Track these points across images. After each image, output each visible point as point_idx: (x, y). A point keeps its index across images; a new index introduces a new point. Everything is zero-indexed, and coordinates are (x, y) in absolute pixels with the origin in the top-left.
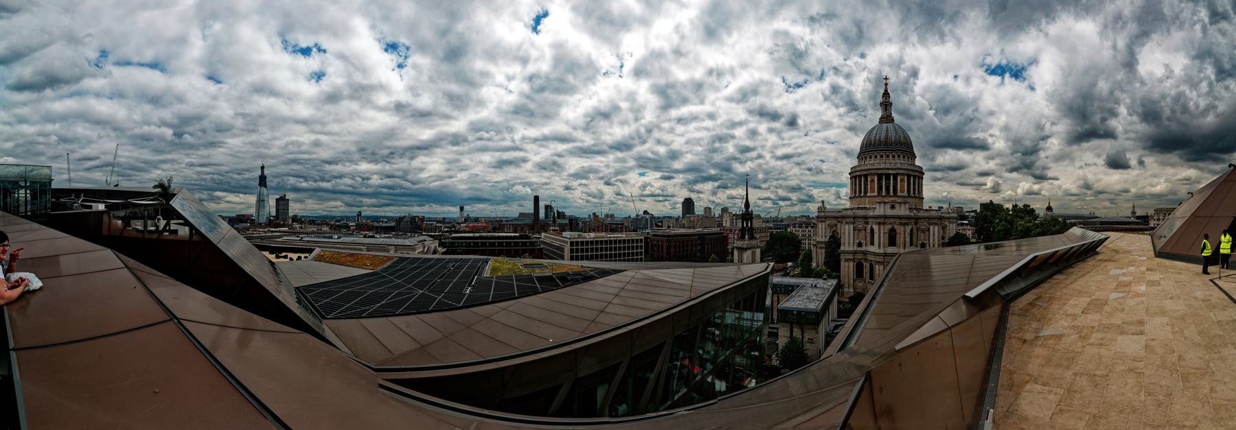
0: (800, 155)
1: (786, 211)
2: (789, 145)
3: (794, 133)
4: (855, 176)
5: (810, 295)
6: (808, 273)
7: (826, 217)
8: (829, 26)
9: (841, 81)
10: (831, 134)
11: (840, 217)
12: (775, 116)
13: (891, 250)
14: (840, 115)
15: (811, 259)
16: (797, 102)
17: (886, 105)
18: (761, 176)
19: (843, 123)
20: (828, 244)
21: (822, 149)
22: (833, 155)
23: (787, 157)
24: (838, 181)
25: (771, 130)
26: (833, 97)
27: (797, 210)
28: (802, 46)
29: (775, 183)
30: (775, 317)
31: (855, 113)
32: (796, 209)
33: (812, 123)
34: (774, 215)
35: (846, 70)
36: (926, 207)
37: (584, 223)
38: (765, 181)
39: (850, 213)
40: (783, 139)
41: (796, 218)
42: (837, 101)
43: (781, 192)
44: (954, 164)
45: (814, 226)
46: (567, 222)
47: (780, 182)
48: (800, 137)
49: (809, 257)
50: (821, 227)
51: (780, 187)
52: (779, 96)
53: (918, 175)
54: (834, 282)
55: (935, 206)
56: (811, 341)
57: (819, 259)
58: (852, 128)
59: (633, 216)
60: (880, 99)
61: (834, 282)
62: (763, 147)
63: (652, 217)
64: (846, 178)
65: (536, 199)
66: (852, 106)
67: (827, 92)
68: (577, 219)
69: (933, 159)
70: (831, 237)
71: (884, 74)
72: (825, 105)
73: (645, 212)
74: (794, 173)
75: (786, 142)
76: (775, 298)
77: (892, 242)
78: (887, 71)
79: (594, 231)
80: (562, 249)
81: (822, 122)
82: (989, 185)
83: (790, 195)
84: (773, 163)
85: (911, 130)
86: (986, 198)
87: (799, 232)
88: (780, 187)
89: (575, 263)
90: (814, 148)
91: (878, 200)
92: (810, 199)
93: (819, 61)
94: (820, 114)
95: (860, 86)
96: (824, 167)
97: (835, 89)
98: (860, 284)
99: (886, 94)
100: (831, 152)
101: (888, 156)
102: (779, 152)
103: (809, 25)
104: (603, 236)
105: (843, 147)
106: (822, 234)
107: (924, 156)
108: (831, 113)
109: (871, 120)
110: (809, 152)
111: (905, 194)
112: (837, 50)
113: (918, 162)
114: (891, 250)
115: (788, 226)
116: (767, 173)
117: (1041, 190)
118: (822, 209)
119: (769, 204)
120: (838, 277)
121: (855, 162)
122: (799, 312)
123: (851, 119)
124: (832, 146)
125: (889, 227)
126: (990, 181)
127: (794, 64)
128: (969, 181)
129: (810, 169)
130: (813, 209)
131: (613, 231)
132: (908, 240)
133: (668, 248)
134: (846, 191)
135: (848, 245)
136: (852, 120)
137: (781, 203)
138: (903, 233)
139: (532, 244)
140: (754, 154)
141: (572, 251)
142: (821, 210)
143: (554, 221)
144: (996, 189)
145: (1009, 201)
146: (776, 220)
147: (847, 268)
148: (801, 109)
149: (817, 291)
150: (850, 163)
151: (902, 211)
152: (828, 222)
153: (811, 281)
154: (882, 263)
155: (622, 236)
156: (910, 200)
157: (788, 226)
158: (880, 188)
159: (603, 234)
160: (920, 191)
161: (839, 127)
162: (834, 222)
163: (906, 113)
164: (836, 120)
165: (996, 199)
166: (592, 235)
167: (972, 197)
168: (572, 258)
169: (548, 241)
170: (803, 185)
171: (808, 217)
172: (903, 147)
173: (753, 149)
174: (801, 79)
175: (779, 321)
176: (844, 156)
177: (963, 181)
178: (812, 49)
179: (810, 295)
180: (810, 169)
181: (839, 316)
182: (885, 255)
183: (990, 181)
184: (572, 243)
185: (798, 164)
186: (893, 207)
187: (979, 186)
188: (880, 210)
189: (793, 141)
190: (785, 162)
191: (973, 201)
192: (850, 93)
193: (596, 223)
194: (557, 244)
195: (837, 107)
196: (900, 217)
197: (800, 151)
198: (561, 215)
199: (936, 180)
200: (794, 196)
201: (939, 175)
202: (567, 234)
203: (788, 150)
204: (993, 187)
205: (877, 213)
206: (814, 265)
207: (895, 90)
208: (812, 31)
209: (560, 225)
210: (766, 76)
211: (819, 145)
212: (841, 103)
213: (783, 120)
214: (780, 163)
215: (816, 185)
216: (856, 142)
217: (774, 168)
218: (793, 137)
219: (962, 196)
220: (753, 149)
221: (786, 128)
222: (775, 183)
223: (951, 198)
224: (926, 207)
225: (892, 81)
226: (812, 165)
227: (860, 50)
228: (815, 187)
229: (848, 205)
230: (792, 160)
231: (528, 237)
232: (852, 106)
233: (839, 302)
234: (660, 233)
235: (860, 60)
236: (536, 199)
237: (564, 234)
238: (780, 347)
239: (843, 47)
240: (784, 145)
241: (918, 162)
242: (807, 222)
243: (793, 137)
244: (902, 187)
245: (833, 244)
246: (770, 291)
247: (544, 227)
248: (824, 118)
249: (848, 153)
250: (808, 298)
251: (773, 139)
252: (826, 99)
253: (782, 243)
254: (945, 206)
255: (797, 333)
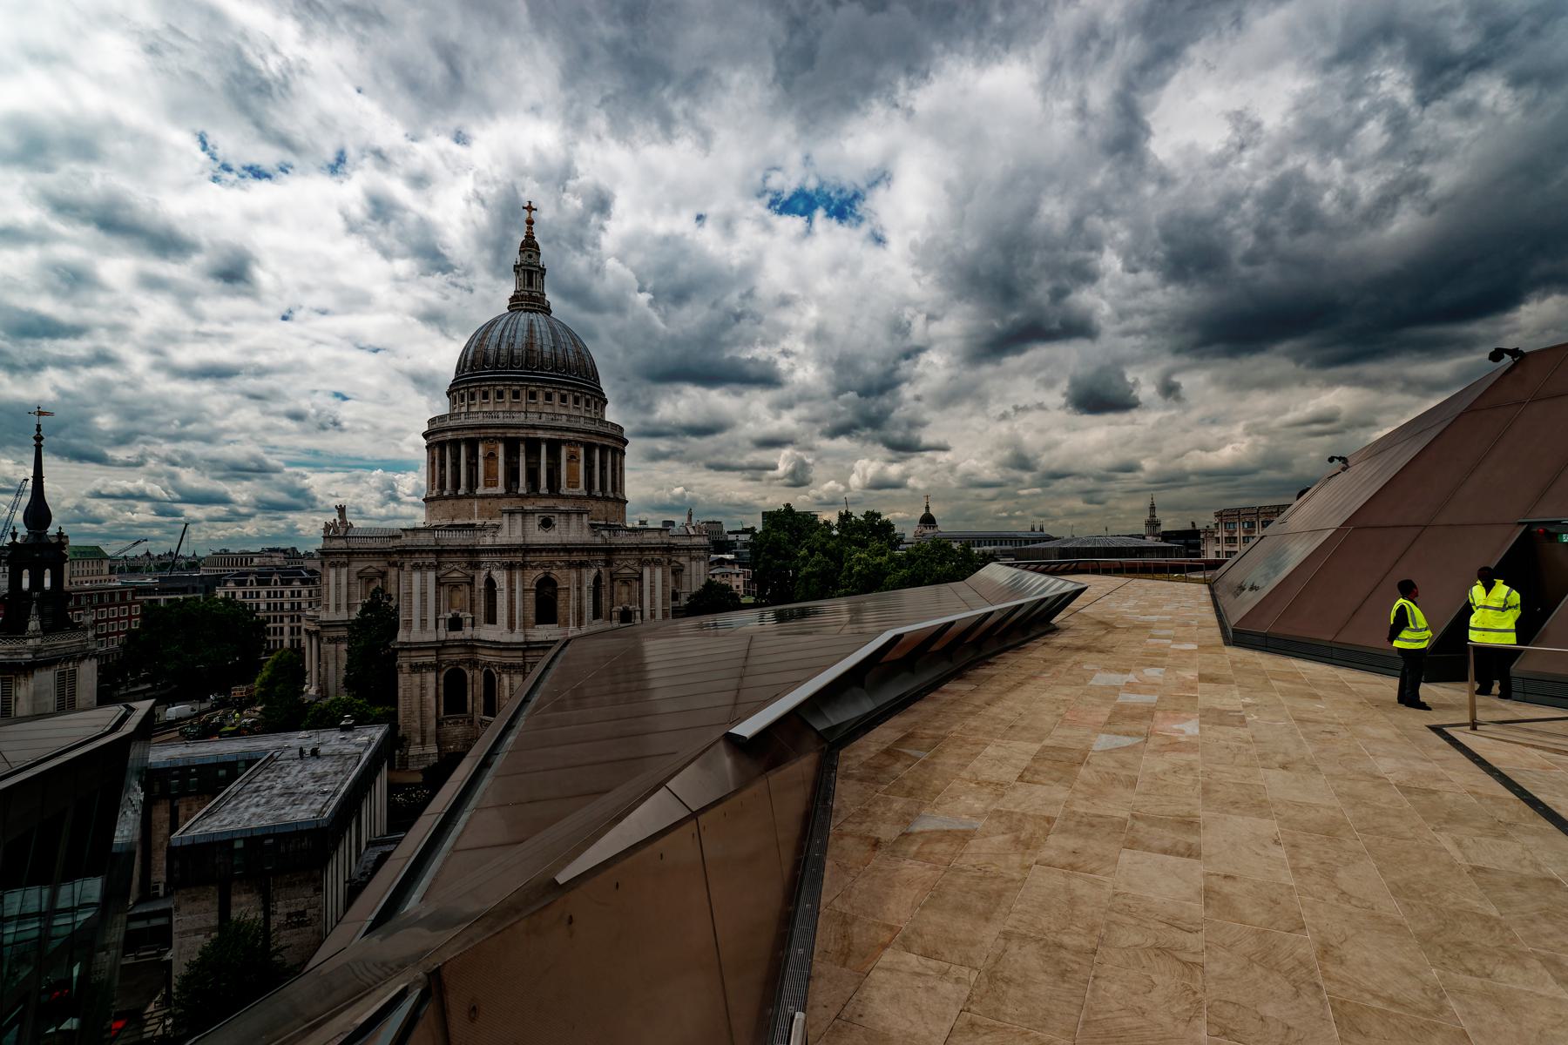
0: (261, 372)
1: (208, 534)
2: (225, 338)
3: (242, 305)
4: (440, 440)
5: (296, 779)
6: (288, 712)
7: (351, 554)
8: (362, 40)
9: (398, 189)
10: (369, 324)
11: (396, 551)
12: (167, 243)
13: (542, 633)
14: (396, 279)
15: (299, 676)
16: (252, 218)
17: (530, 271)
18: (105, 421)
19: (405, 301)
20: (356, 629)
21: (341, 363)
22: (373, 381)
23: (216, 373)
24: (390, 454)
25: (152, 284)
26: (374, 227)
27: (253, 532)
28: (272, 66)
29: (166, 448)
30: (160, 876)
31: (438, 279)
32: (250, 528)
33: (306, 289)
34: (159, 548)
35: (416, 164)
36: (632, 521)
38: (123, 439)
39: (424, 540)
40: (199, 318)
41: (247, 557)
42: (384, 239)
43: (189, 478)
44: (699, 419)
45: (312, 578)
47: (184, 446)
48: (263, 320)
49: (292, 668)
50: (336, 581)
51: (188, 460)
52: (186, 186)
53: (612, 444)
54: (377, 733)
55: (655, 521)
56: (298, 920)
57: (324, 673)
58: (433, 318)
60: (514, 256)
61: (377, 733)
62: (117, 329)
64: (415, 447)
66: (432, 257)
67: (357, 211)
69: (649, 409)
70: (366, 608)
71: (525, 197)
72: (352, 244)
74: (241, 425)
75: (217, 328)
76: (161, 814)
77: (546, 610)
78: (531, 191)
81: (339, 289)
82: (783, 467)
83: (222, 487)
84: (159, 385)
85: (593, 336)
86: (775, 499)
87: (261, 599)
88: (188, 460)
90: (314, 356)
91: (506, 505)
92: (302, 500)
93: (327, 122)
94: (330, 266)
95: (455, 214)
96: (346, 412)
97: (381, 208)
98: (458, 731)
99: (529, 245)
100: (365, 373)
101: (530, 396)
102: (186, 355)
103: (297, 17)
105: (407, 365)
106: (339, 598)
107: (626, 400)
108: (366, 268)
109: (486, 301)
110: (296, 368)
111: (581, 489)
112: (388, 108)
113: (611, 415)
114: (542, 633)
115: (219, 580)
116: (131, 412)
117: (906, 476)
118: (339, 529)
119: (143, 513)
120: (391, 718)
121: (442, 406)
122: (255, 841)
123: (430, 291)
124: (372, 359)
125: (539, 573)
126: (784, 460)
127: (244, 108)
128: (734, 460)
129: (297, 416)
130: (309, 529)
132: (588, 603)
134: (413, 482)
135: (420, 624)
136: (433, 297)
137: (191, 511)
138: (575, 586)
140: (77, 348)
142: (330, 532)
144: (799, 478)
145: (831, 504)
146: (168, 563)
147: (418, 691)
148: (262, 240)
149: (318, 767)
150: (424, 408)
151: (572, 532)
152: (357, 566)
153: (298, 739)
154: (522, 669)
156: (593, 506)
157: (219, 580)
158: (512, 475)
160: (618, 484)
161: (392, 309)
162: (378, 564)
163: (579, 295)
164: (382, 291)
165: (801, 501)
167: (743, 498)
170: (272, 461)
171: (292, 554)
172: (576, 377)
173: (76, 331)
174: (267, 156)
175: (173, 886)
176: (410, 389)
177: (721, 459)
178: (301, 84)
179: (296, 779)
180: (297, 416)
181: (390, 831)
182: (528, 647)
183: (784, 460)
185: (255, 397)
186: (546, 524)
187: (758, 471)
188: (511, 533)
189: (235, 328)
190: (206, 386)
191: (745, 507)
192: (424, 225)
195: (387, 254)
196: (567, 549)
197: (263, 359)
199: (656, 456)
200: (242, 492)
201: (662, 445)
203: (222, 354)
204: (793, 474)
205: (503, 538)
206: (311, 691)
207: (553, 239)
208: (308, 33)
210: (134, 114)
211: (329, 352)
212: (399, 247)
213: (198, 260)
214: (184, 390)
215: (318, 461)
216: (445, 356)
217: (165, 403)
218: (239, 318)
219: (720, 497)
220: (76, 331)
221: (213, 285)
222: (166, 448)
223: (694, 501)
224: (632, 521)
225: (545, 215)
226: (304, 404)
227: (456, 121)
228: (318, 467)
229: (420, 517)
230: (235, 383)
232: (432, 257)
233: (393, 788)
235: (457, 149)
238: (179, 970)
239: (404, 102)
240: (205, 336)
241: (611, 415)
242: (287, 567)
243: (239, 318)
244: (572, 473)
245: (375, 628)
246: (138, 796)
248: (346, 279)
249: (420, 381)
250: (288, 792)
251: (157, 312)
252: (352, 228)
253: (200, 633)
254: (679, 519)
255: (246, 908)
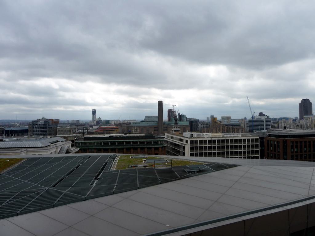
37: (203, 123)
46: (187, 123)
59: (249, 117)
63: (268, 120)
65: (160, 104)
68: (197, 121)
73: (261, 114)
79: (212, 131)
80: (183, 148)
89: (194, 158)
104: (219, 136)
131: (228, 131)
133: (285, 148)
139: (156, 143)
141: (192, 149)
143: (176, 123)
155: (238, 136)
159: (220, 134)
166: (210, 135)
168: (192, 155)
169: (170, 140)
184: (192, 142)
193: (213, 125)
194: (178, 143)
198: (181, 117)
202: (187, 134)
209: (181, 127)
231: (153, 137)
234: (276, 133)
236: (160, 104)
237: (185, 134)
247: (166, 128)
